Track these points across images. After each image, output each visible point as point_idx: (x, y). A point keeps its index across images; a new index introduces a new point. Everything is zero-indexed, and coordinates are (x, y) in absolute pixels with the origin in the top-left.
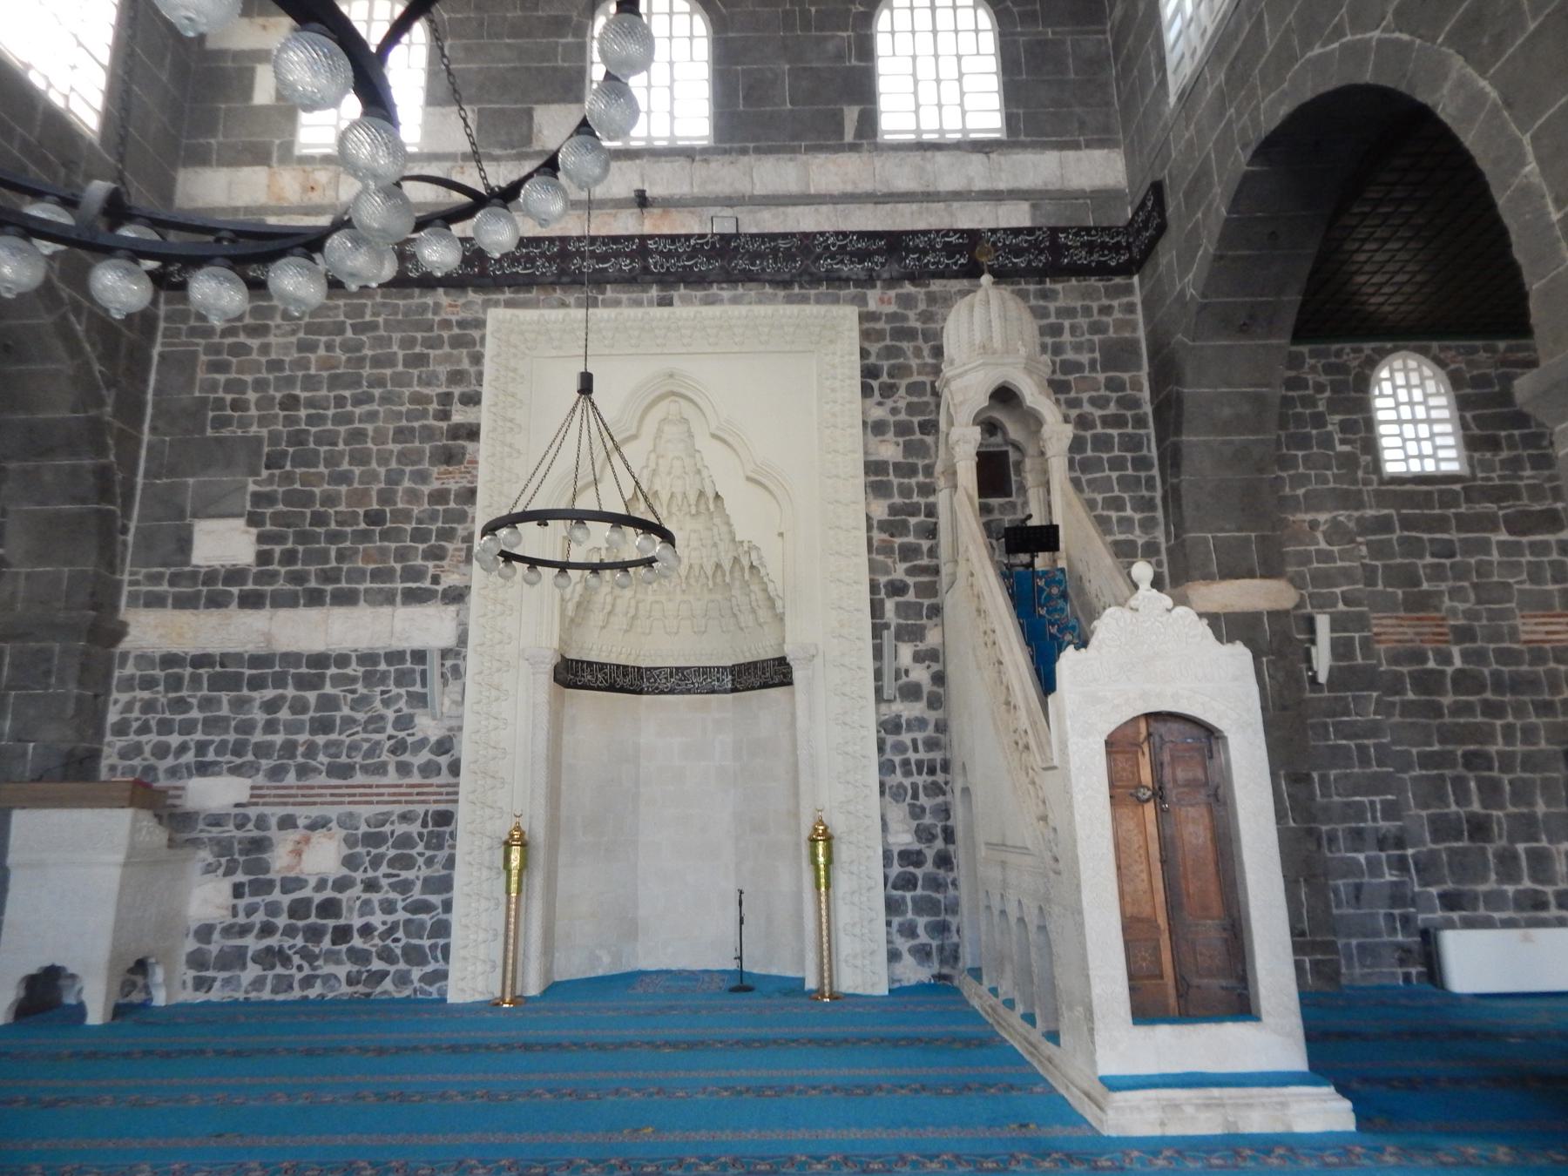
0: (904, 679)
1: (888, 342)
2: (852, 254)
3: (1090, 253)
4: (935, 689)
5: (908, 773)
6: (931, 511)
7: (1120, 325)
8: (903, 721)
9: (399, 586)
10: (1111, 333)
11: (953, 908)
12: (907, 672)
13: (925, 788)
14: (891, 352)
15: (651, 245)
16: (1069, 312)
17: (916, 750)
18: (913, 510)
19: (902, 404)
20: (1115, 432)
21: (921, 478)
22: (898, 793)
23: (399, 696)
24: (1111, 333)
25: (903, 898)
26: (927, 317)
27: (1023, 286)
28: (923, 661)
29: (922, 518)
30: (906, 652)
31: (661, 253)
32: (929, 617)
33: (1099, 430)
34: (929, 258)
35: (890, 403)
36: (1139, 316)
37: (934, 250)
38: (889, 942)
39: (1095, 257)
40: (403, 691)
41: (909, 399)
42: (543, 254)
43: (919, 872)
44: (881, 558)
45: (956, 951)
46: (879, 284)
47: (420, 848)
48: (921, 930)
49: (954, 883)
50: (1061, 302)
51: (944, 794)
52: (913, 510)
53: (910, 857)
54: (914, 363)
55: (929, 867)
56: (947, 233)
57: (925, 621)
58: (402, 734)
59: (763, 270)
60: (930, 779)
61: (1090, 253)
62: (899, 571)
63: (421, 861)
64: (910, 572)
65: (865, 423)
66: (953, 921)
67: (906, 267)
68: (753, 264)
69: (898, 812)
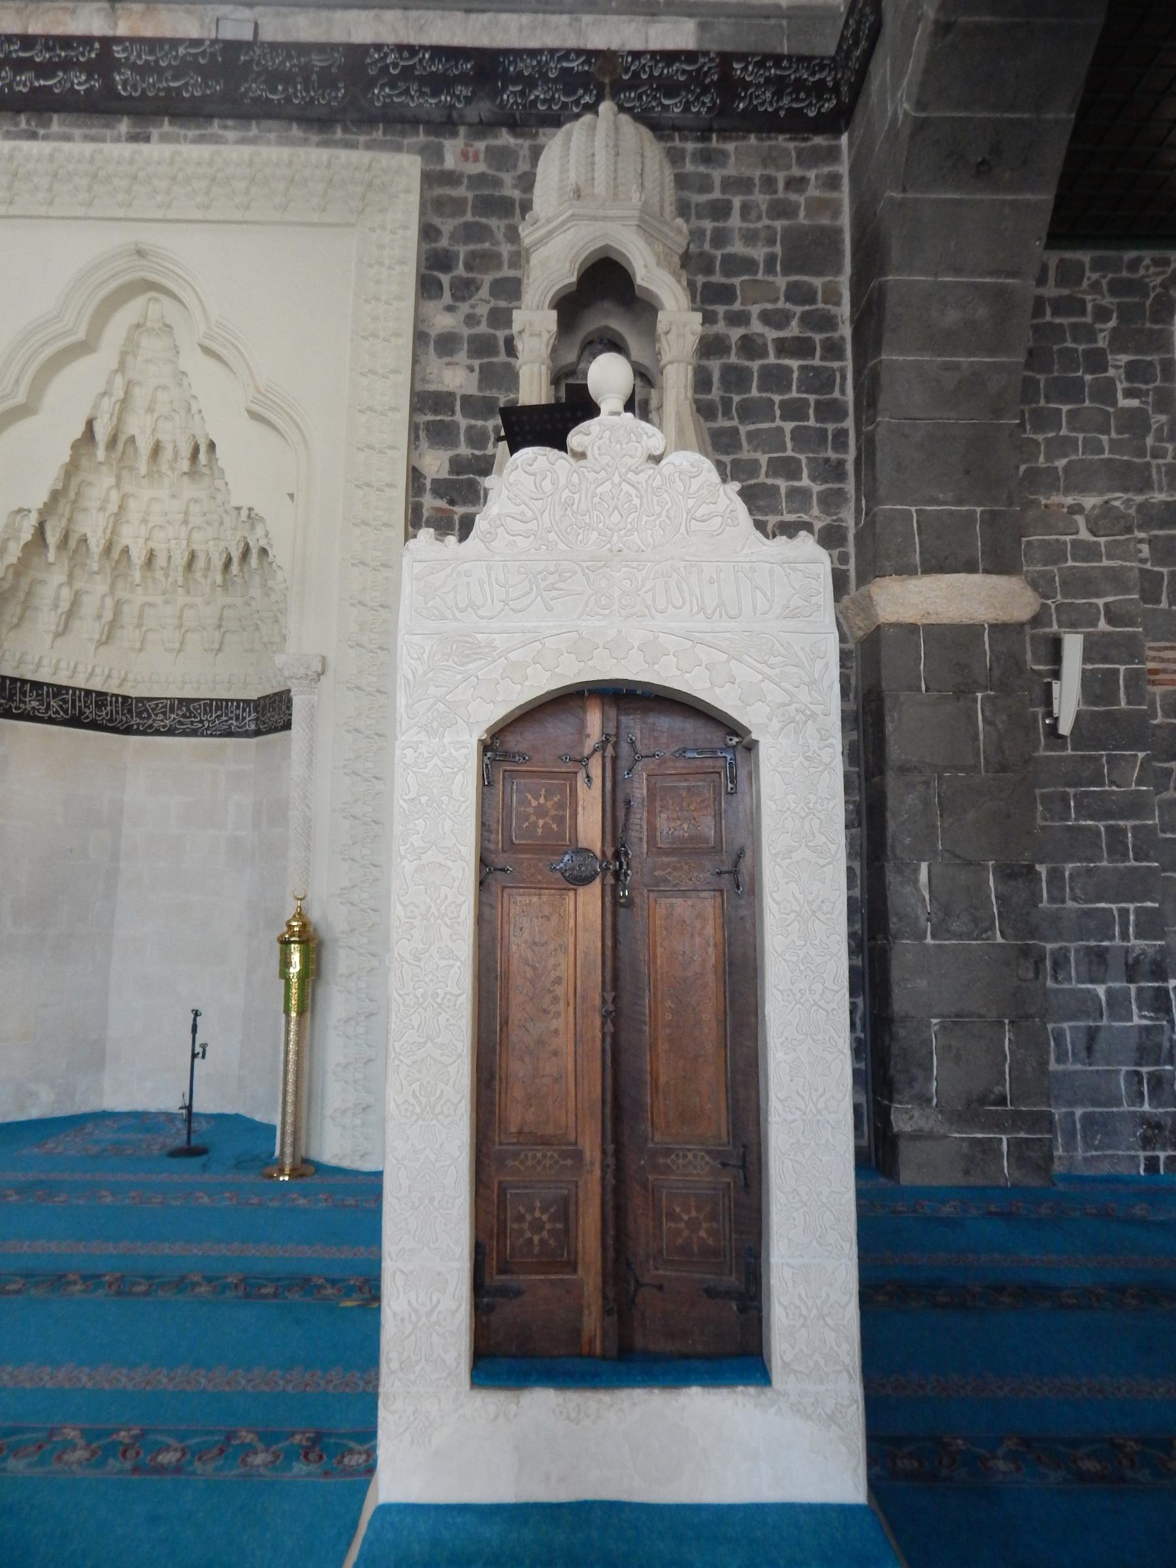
1: (469, 217)
3: (779, 94)
7: (816, 206)
10: (802, 218)
14: (473, 232)
16: (743, 185)
19: (482, 310)
20: (794, 364)
24: (802, 218)
27: (677, 143)
33: (772, 359)
34: (539, 93)
35: (464, 308)
36: (845, 195)
37: (544, 77)
39: (786, 101)
41: (493, 303)
46: (462, 130)
50: (731, 170)
54: (505, 249)
56: (567, 54)
61: (779, 94)
67: (502, 106)
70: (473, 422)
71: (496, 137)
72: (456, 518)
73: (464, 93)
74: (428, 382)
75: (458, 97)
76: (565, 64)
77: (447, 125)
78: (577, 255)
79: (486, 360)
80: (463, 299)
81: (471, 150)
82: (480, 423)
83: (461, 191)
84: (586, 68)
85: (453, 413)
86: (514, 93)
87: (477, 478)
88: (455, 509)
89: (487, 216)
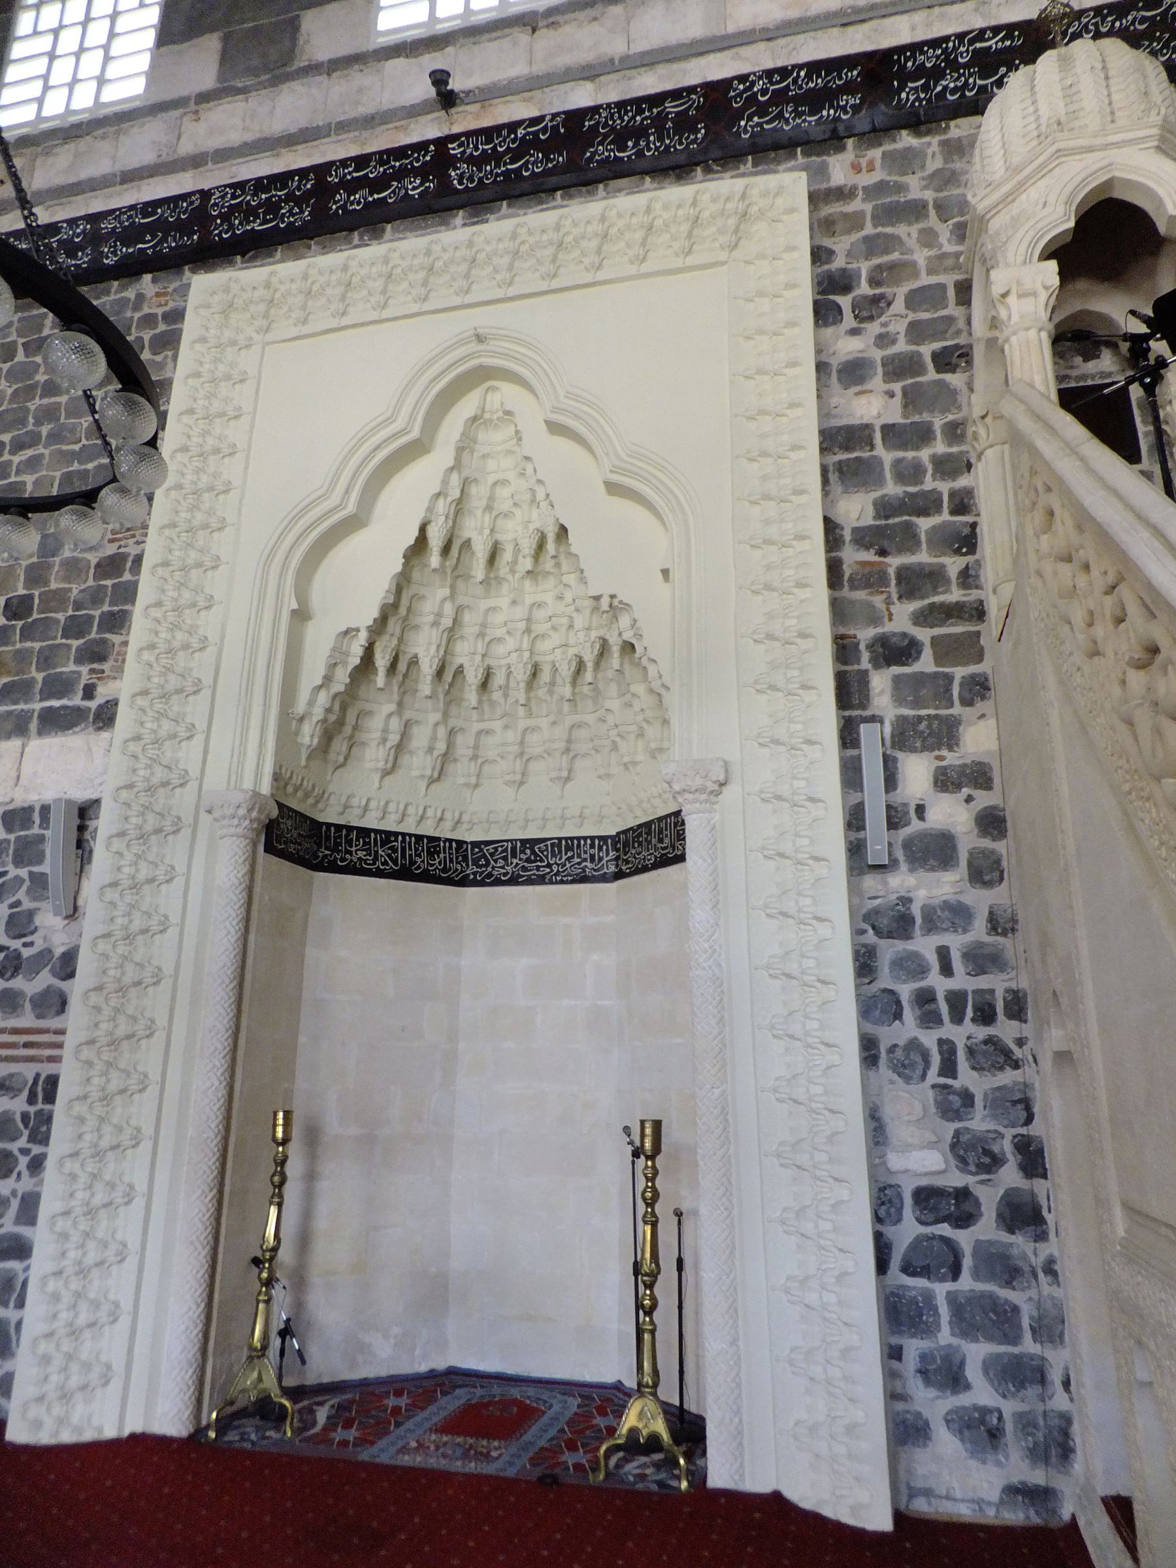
0: (915, 826)
1: (869, 230)
2: (798, 100)
4: (986, 843)
5: (930, 1019)
6: (963, 503)
8: (916, 910)
9: (37, 706)
11: (1050, 1328)
12: (920, 810)
13: (971, 1052)
15: (454, 149)
17: (947, 969)
18: (927, 505)
19: (899, 327)
21: (940, 447)
22: (909, 1062)
23: (19, 880)
25: (929, 1297)
26: (946, 179)
28: (958, 787)
29: (945, 516)
30: (917, 772)
31: (471, 160)
32: (967, 702)
35: (874, 328)
37: (954, 65)
38: (894, 1396)
40: (23, 872)
42: (290, 197)
43: (965, 1238)
44: (860, 595)
45: (1066, 1433)
46: (850, 143)
47: (22, 1142)
48: (973, 1372)
49: (1050, 1269)
51: (1016, 1065)
52: (927, 505)
53: (946, 1205)
54: (921, 257)
55: (987, 1228)
57: (957, 710)
58: (16, 944)
59: (640, 154)
60: (982, 1033)
62: (901, 618)
63: (23, 1161)
64: (922, 618)
65: (821, 368)
66: (1057, 1360)
67: (900, 106)
68: (623, 148)
69: (909, 1104)
70: (900, 454)
71: (894, 141)
72: (891, 572)
73: (852, 102)
74: (835, 416)
75: (844, 109)
76: (978, 45)
77: (833, 140)
78: (1072, 195)
79: (910, 381)
80: (871, 318)
81: (864, 162)
82: (910, 454)
83: (857, 205)
84: (1008, 43)
85: (872, 448)
86: (916, 89)
87: (914, 519)
88: (888, 560)
89: (893, 225)
